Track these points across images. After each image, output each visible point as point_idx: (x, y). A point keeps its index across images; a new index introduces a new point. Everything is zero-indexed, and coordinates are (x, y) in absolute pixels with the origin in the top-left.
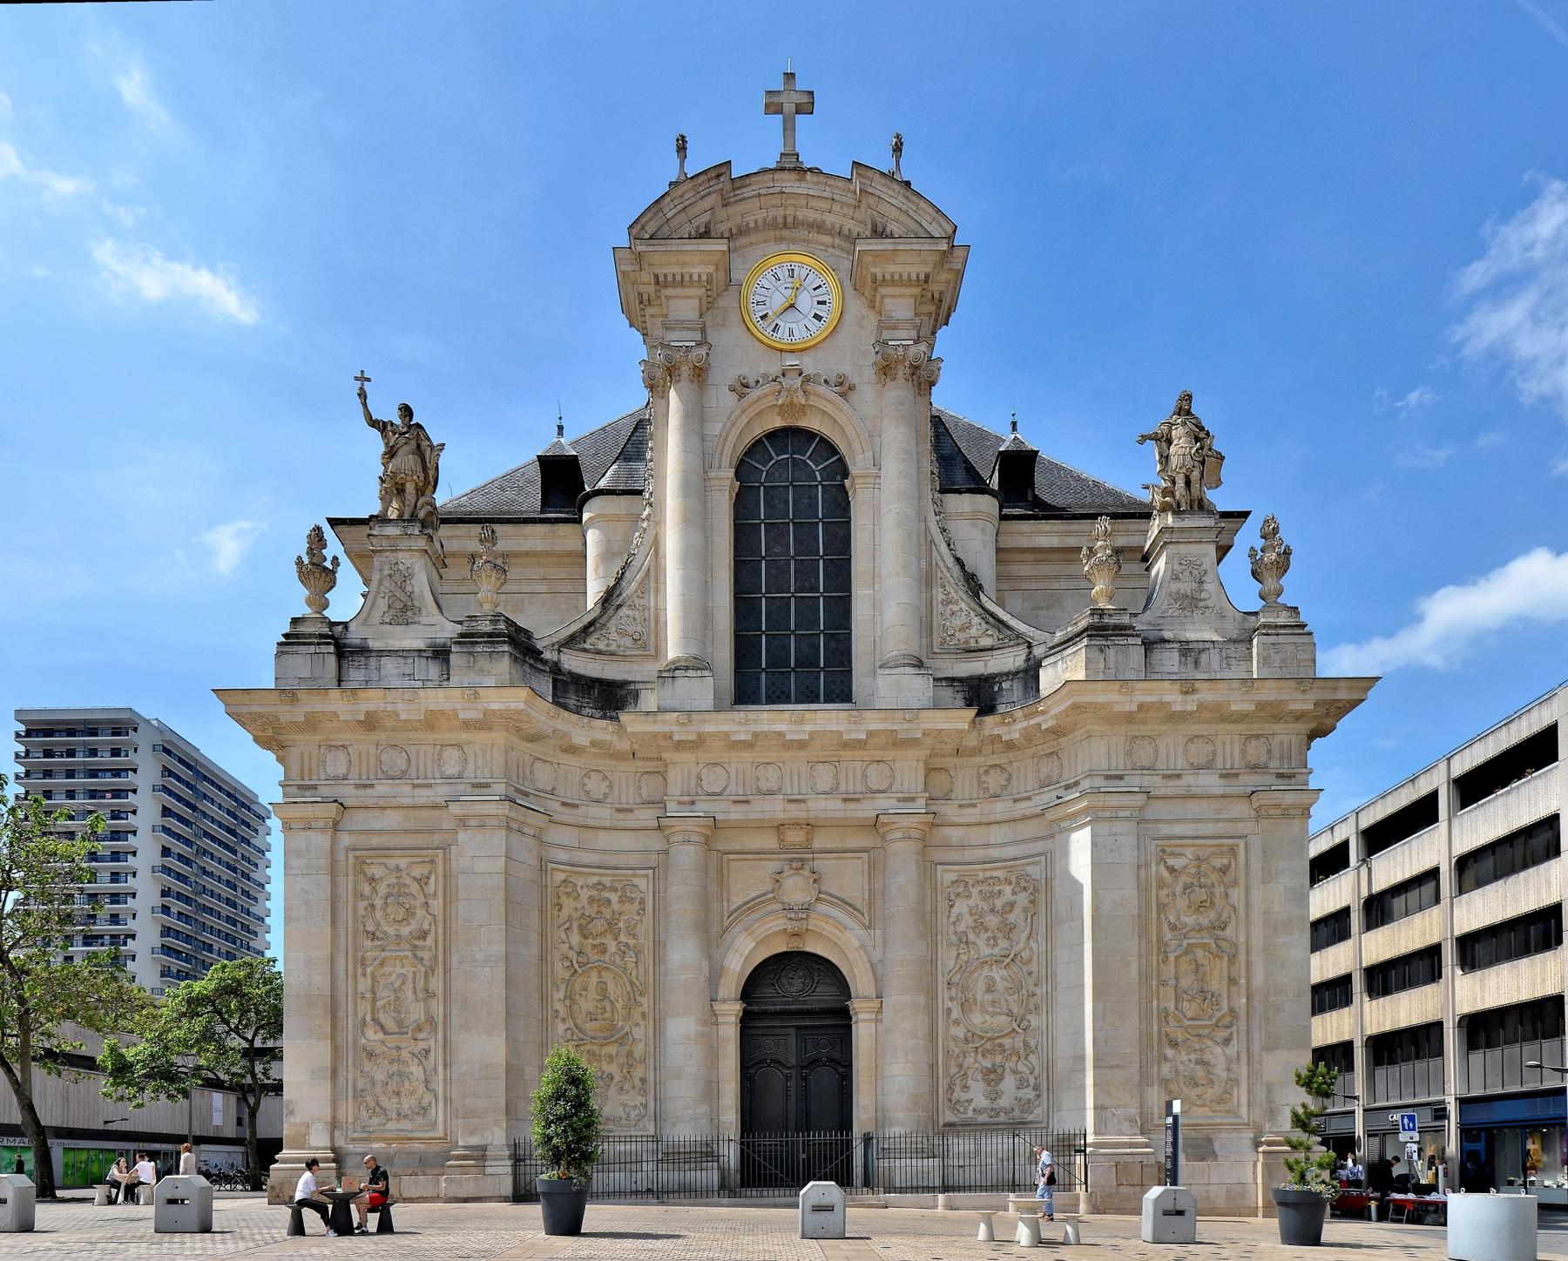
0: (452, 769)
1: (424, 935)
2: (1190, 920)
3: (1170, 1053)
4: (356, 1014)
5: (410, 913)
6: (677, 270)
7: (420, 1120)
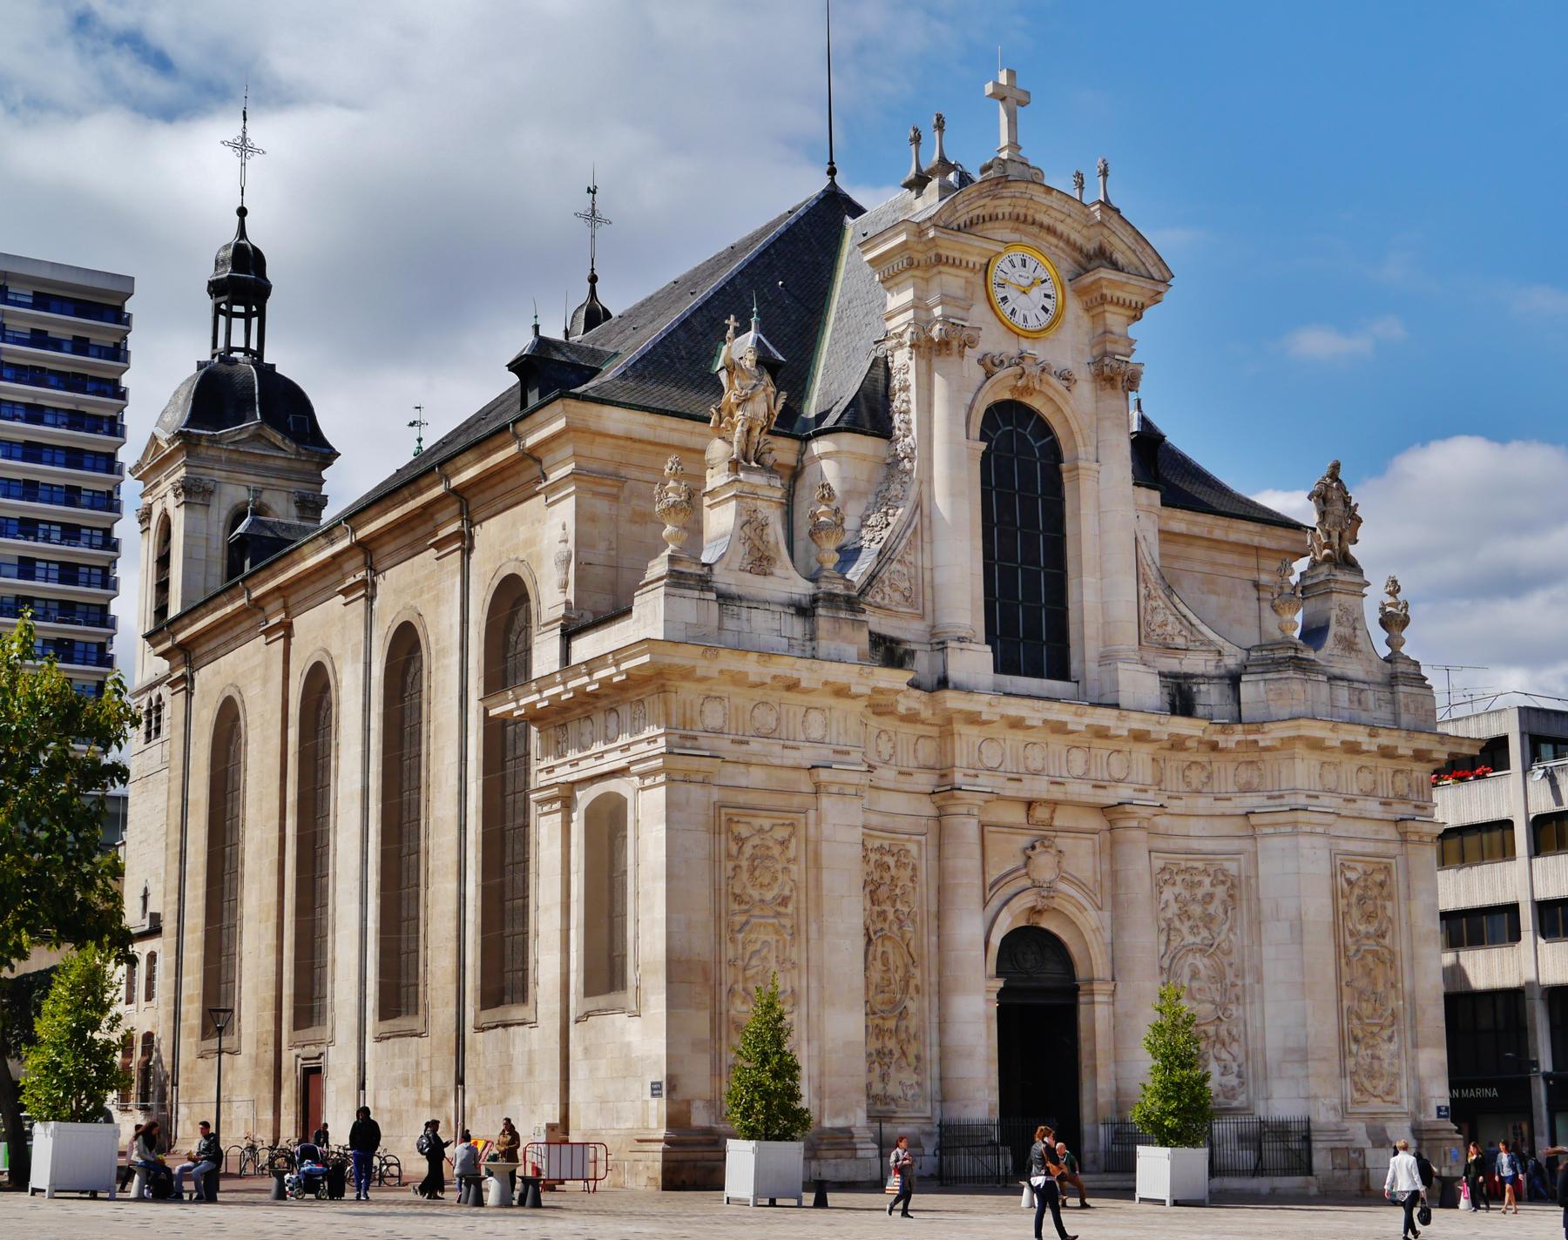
0: (816, 733)
1: (784, 901)
2: (1362, 928)
3: (1354, 1047)
6: (957, 255)
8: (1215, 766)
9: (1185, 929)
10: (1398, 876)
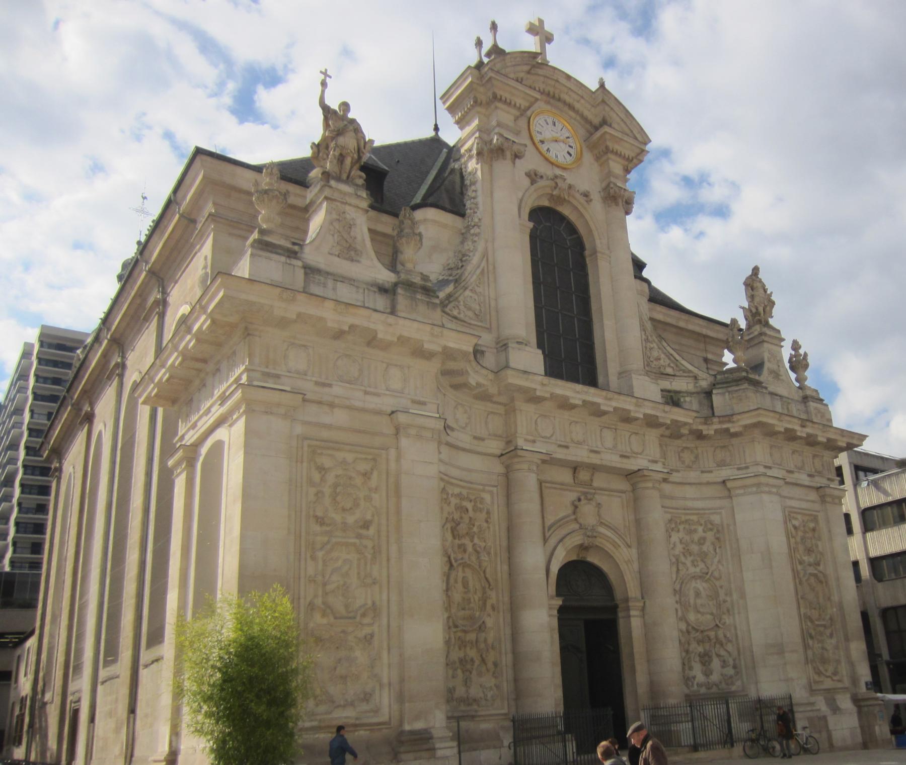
0: (396, 384)
1: (366, 525)
2: (805, 558)
3: (811, 642)
4: (305, 598)
5: (356, 504)
7: (364, 707)
8: (700, 450)
9: (689, 563)
10: (822, 525)
